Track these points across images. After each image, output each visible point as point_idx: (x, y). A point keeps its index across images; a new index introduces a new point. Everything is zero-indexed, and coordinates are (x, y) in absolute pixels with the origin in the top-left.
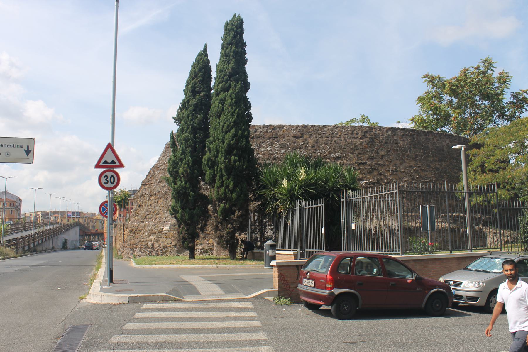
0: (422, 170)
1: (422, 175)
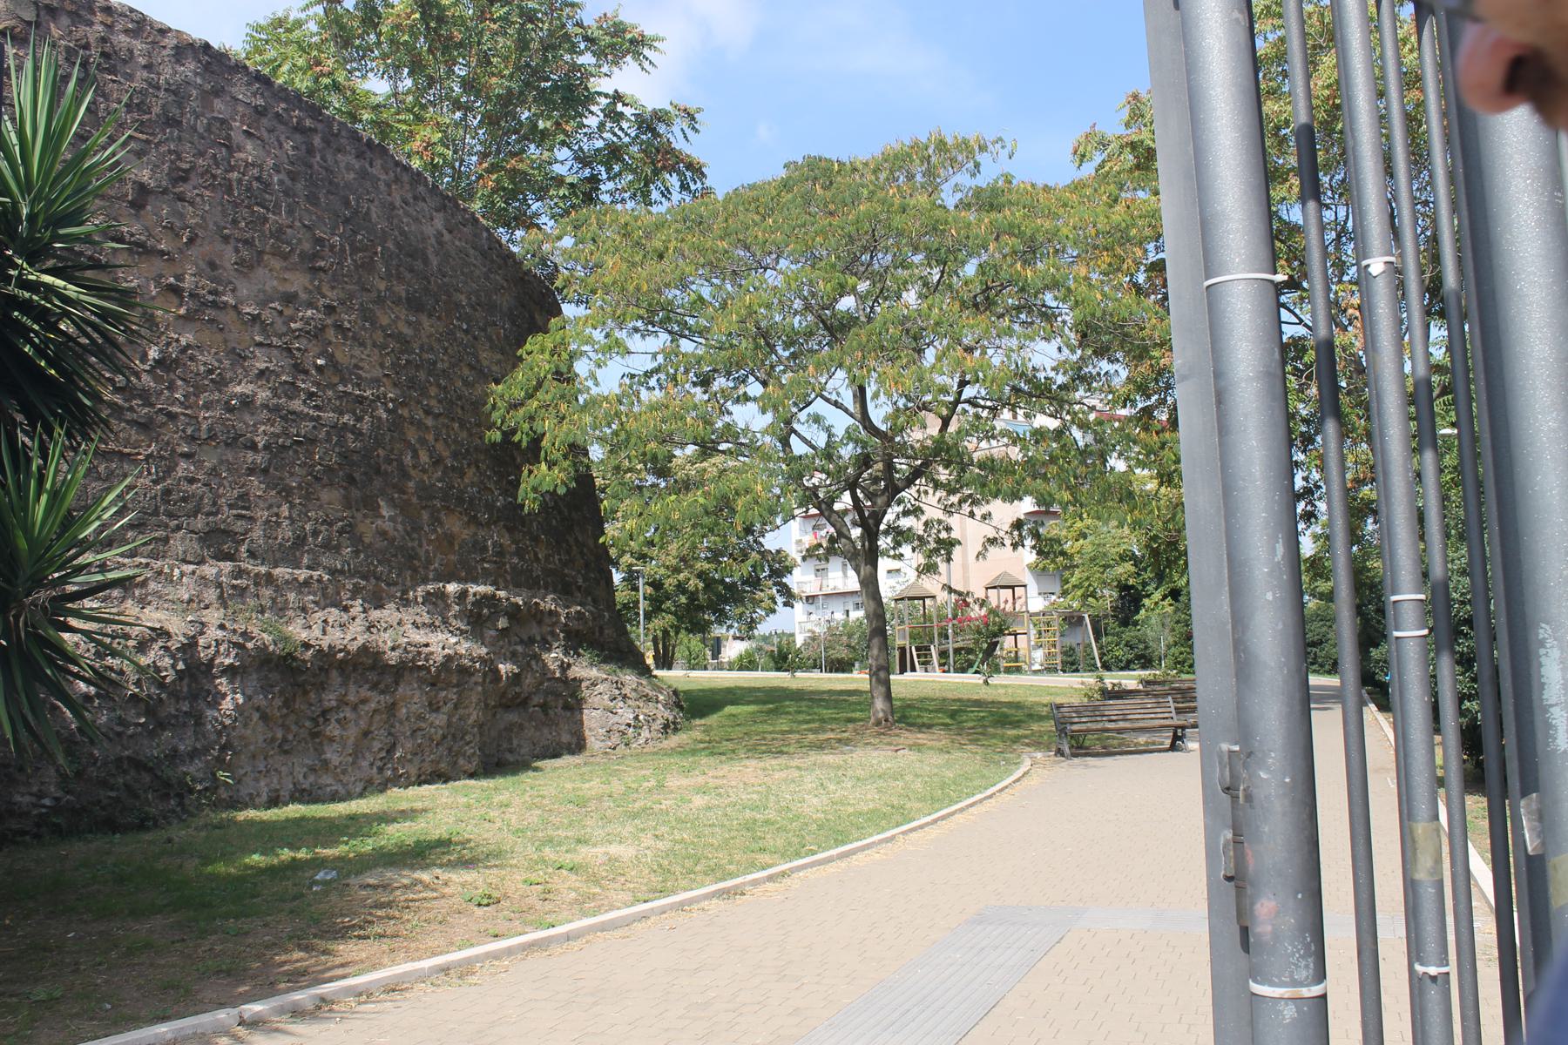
0: (339, 327)
1: (339, 356)
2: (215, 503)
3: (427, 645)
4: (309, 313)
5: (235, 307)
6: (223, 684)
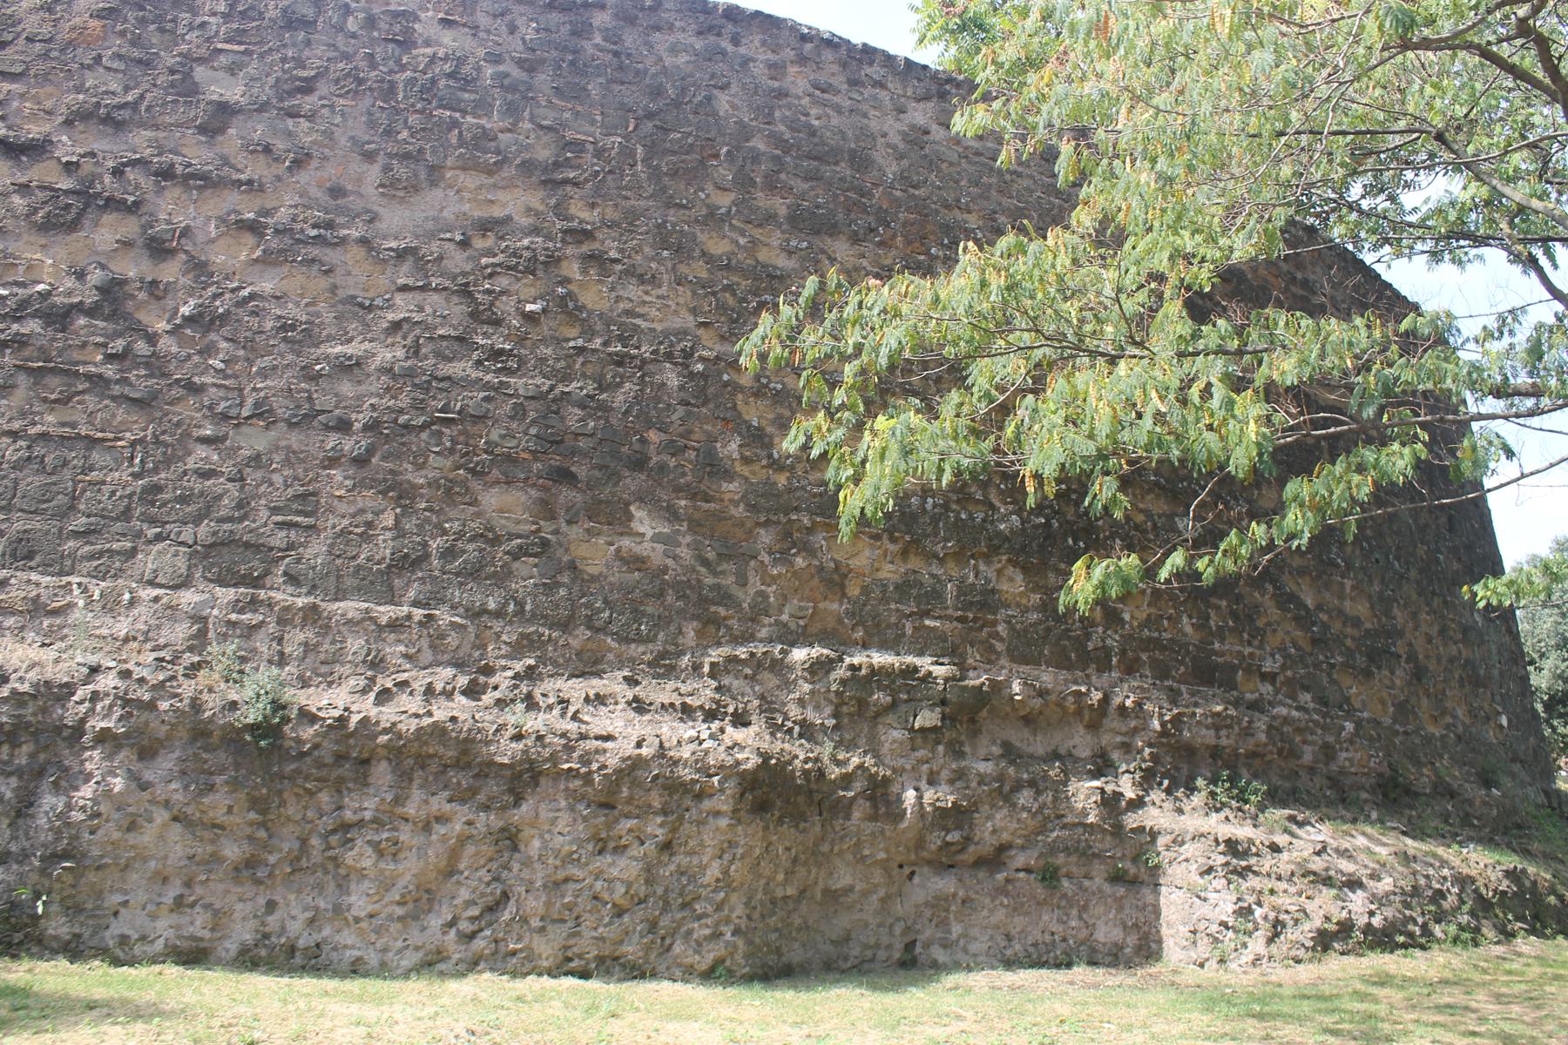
2: (240, 506)
3: (609, 738)
4: (526, 242)
5: (363, 241)
6: (94, 760)
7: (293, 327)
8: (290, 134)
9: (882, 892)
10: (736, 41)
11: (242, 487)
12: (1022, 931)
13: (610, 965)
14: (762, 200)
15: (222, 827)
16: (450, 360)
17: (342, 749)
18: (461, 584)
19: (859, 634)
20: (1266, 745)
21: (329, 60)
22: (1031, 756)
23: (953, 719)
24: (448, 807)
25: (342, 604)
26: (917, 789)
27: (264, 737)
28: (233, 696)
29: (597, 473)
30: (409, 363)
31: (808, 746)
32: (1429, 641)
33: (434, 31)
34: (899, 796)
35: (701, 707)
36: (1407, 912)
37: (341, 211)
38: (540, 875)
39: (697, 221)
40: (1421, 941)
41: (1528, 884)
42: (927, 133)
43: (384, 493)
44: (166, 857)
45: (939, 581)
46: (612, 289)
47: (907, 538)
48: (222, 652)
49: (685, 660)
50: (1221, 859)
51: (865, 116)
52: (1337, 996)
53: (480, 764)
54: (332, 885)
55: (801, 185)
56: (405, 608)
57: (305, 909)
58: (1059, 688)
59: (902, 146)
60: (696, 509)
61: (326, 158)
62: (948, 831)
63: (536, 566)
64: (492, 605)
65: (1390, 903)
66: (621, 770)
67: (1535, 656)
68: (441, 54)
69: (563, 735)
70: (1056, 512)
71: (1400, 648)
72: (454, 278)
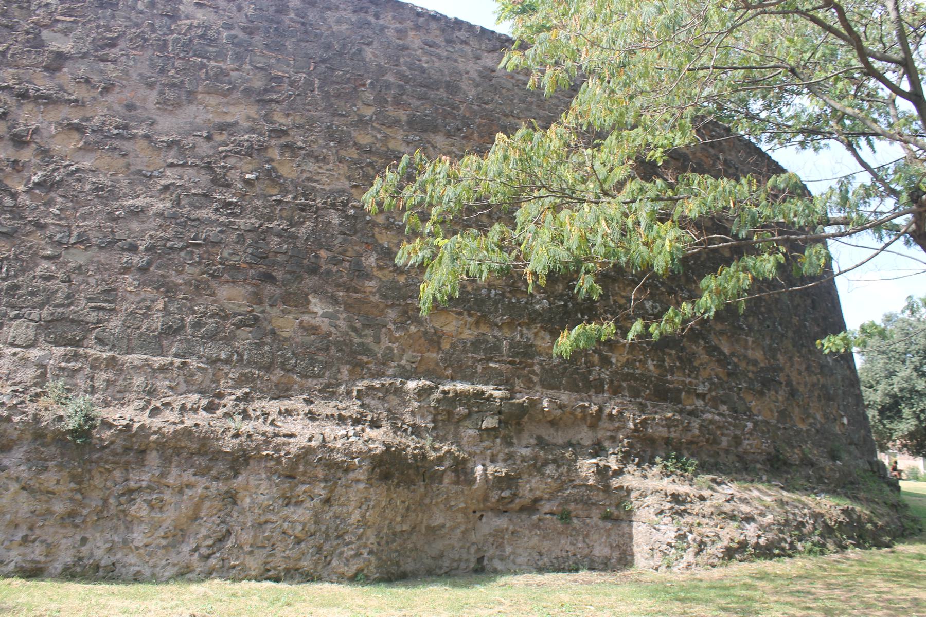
0: (289, 147)
2: (68, 297)
3: (292, 436)
4: (246, 137)
5: (147, 137)
7: (102, 189)
8: (101, 72)
9: (463, 528)
10: (377, 16)
11: (70, 286)
12: (549, 550)
13: (293, 574)
14: (392, 111)
15: (53, 493)
16: (199, 208)
17: (128, 444)
18: (204, 343)
19: (449, 372)
20: (699, 436)
21: (126, 27)
22: (555, 445)
23: (506, 423)
24: (193, 479)
25: (130, 356)
26: (483, 465)
27: (79, 437)
28: (61, 412)
29: (288, 276)
30: (174, 210)
31: (416, 440)
32: (800, 374)
33: (191, 9)
34: (473, 469)
35: (351, 417)
36: (781, 535)
37: (132, 118)
38: (250, 519)
39: (351, 124)
40: (790, 553)
41: (855, 517)
42: (494, 71)
43: (157, 289)
44: (17, 512)
45: (498, 340)
46: (299, 165)
47: (479, 314)
48: (55, 386)
49: (342, 388)
50: (669, 505)
51: (456, 61)
52: (733, 587)
53: (213, 453)
54: (123, 527)
55: (415, 103)
56: (170, 359)
57: (106, 542)
58: (572, 404)
59: (478, 79)
60: (348, 296)
61: (124, 87)
62: (503, 491)
63: (250, 332)
64: (223, 356)
65: (771, 530)
66: (299, 455)
67: (874, 383)
68: (195, 24)
69: (264, 434)
70: (571, 298)
71: (782, 378)
72: (202, 159)
